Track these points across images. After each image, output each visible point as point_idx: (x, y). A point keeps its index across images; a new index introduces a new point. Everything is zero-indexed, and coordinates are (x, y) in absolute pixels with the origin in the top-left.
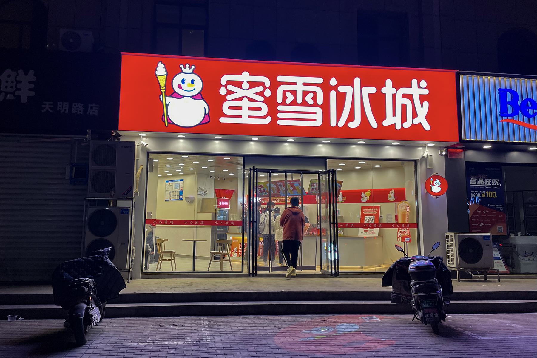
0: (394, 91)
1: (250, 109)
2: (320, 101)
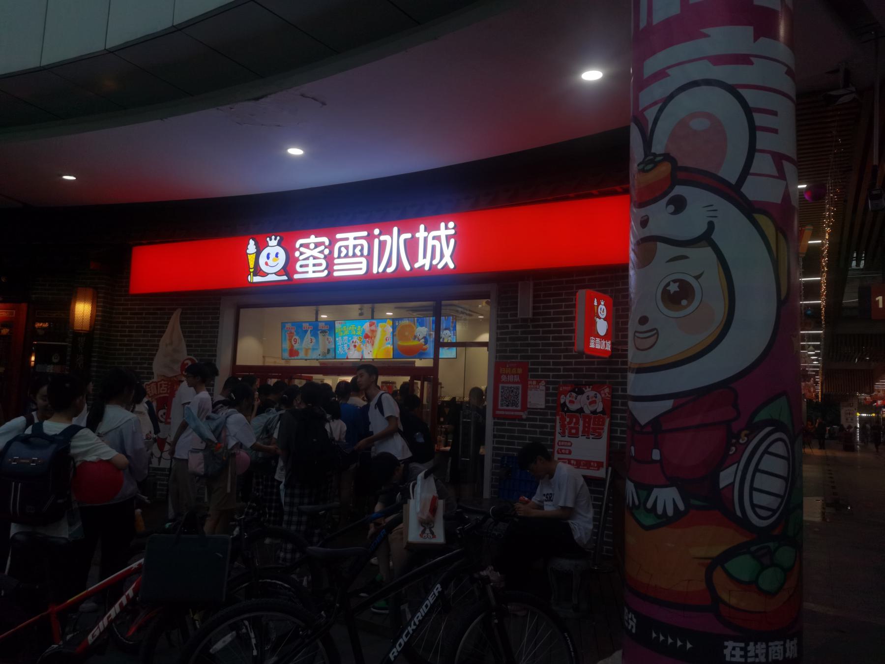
0: (426, 234)
1: (314, 265)
2: (366, 253)
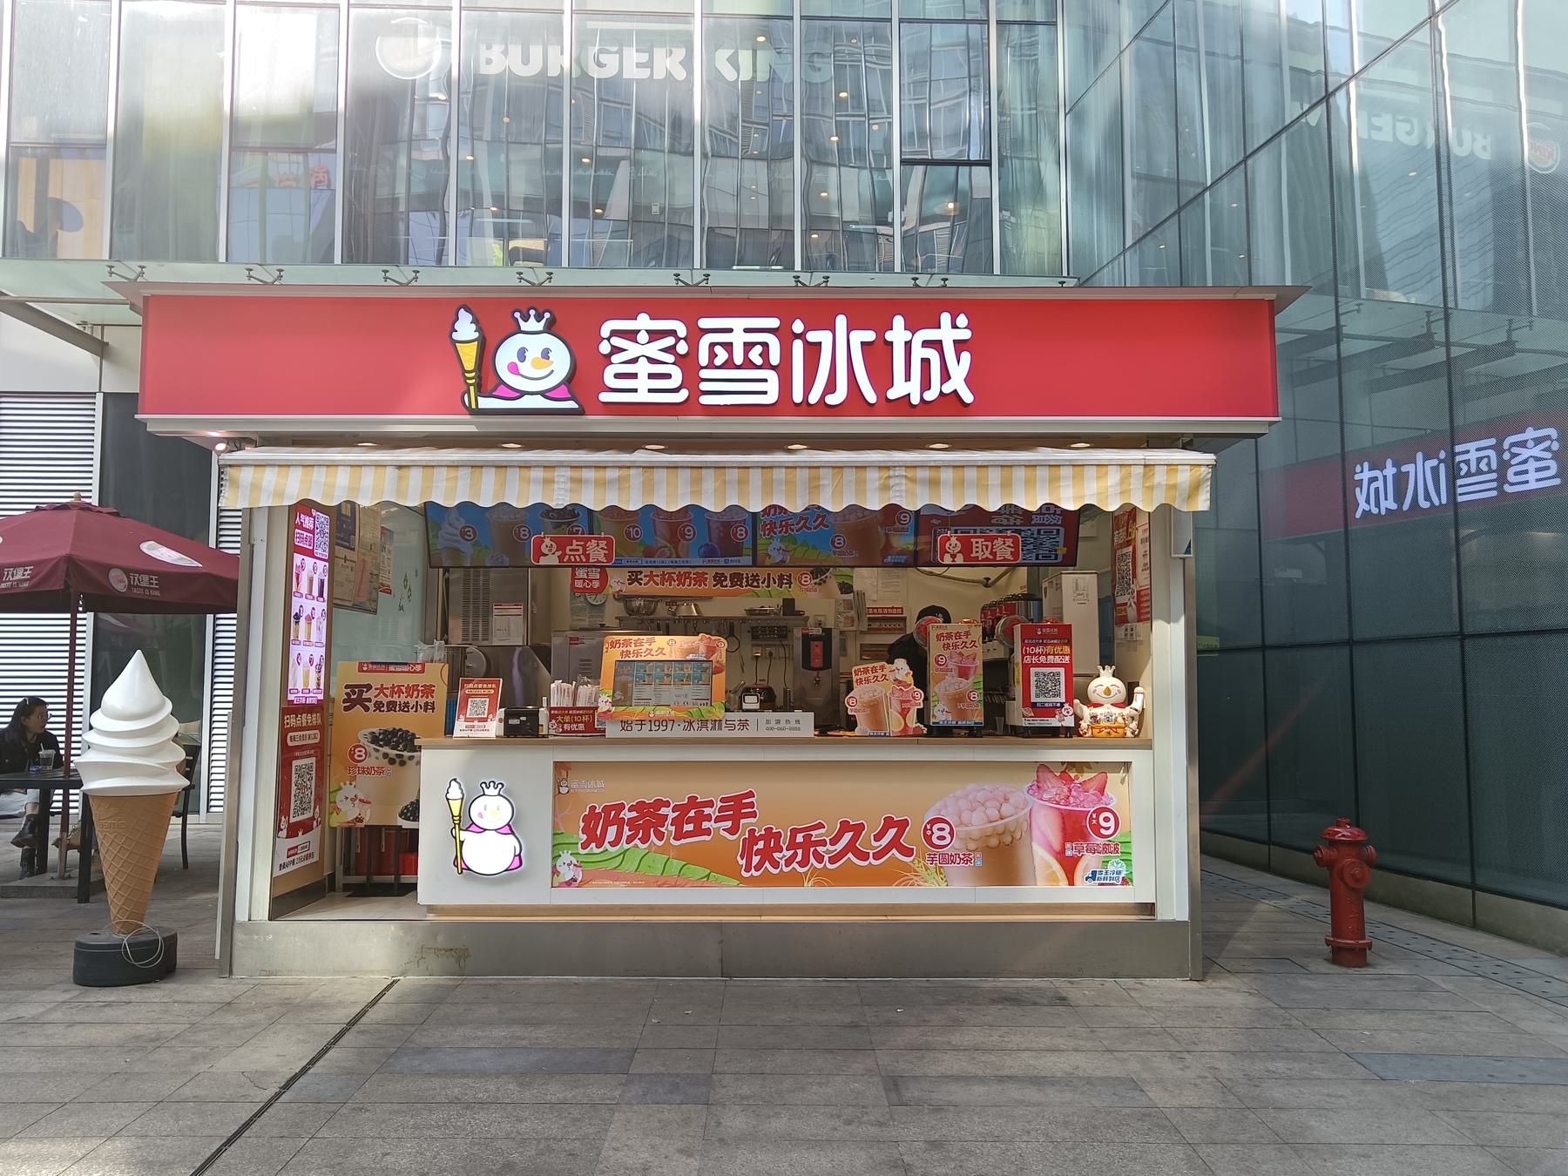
0: (907, 335)
1: (652, 376)
2: (775, 359)
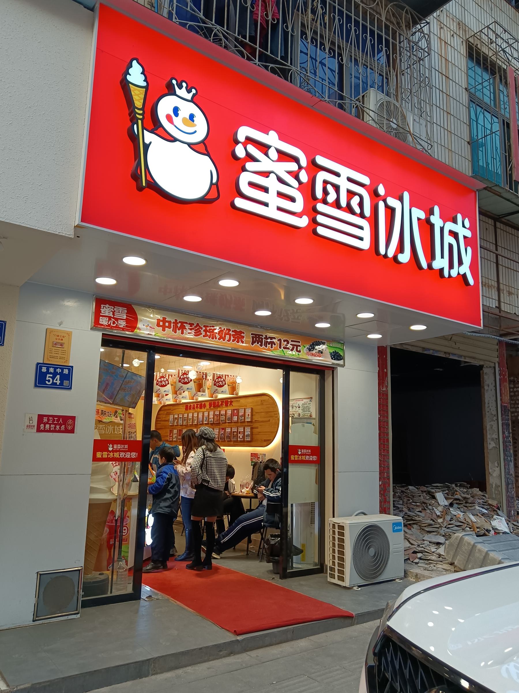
1: (280, 195)
